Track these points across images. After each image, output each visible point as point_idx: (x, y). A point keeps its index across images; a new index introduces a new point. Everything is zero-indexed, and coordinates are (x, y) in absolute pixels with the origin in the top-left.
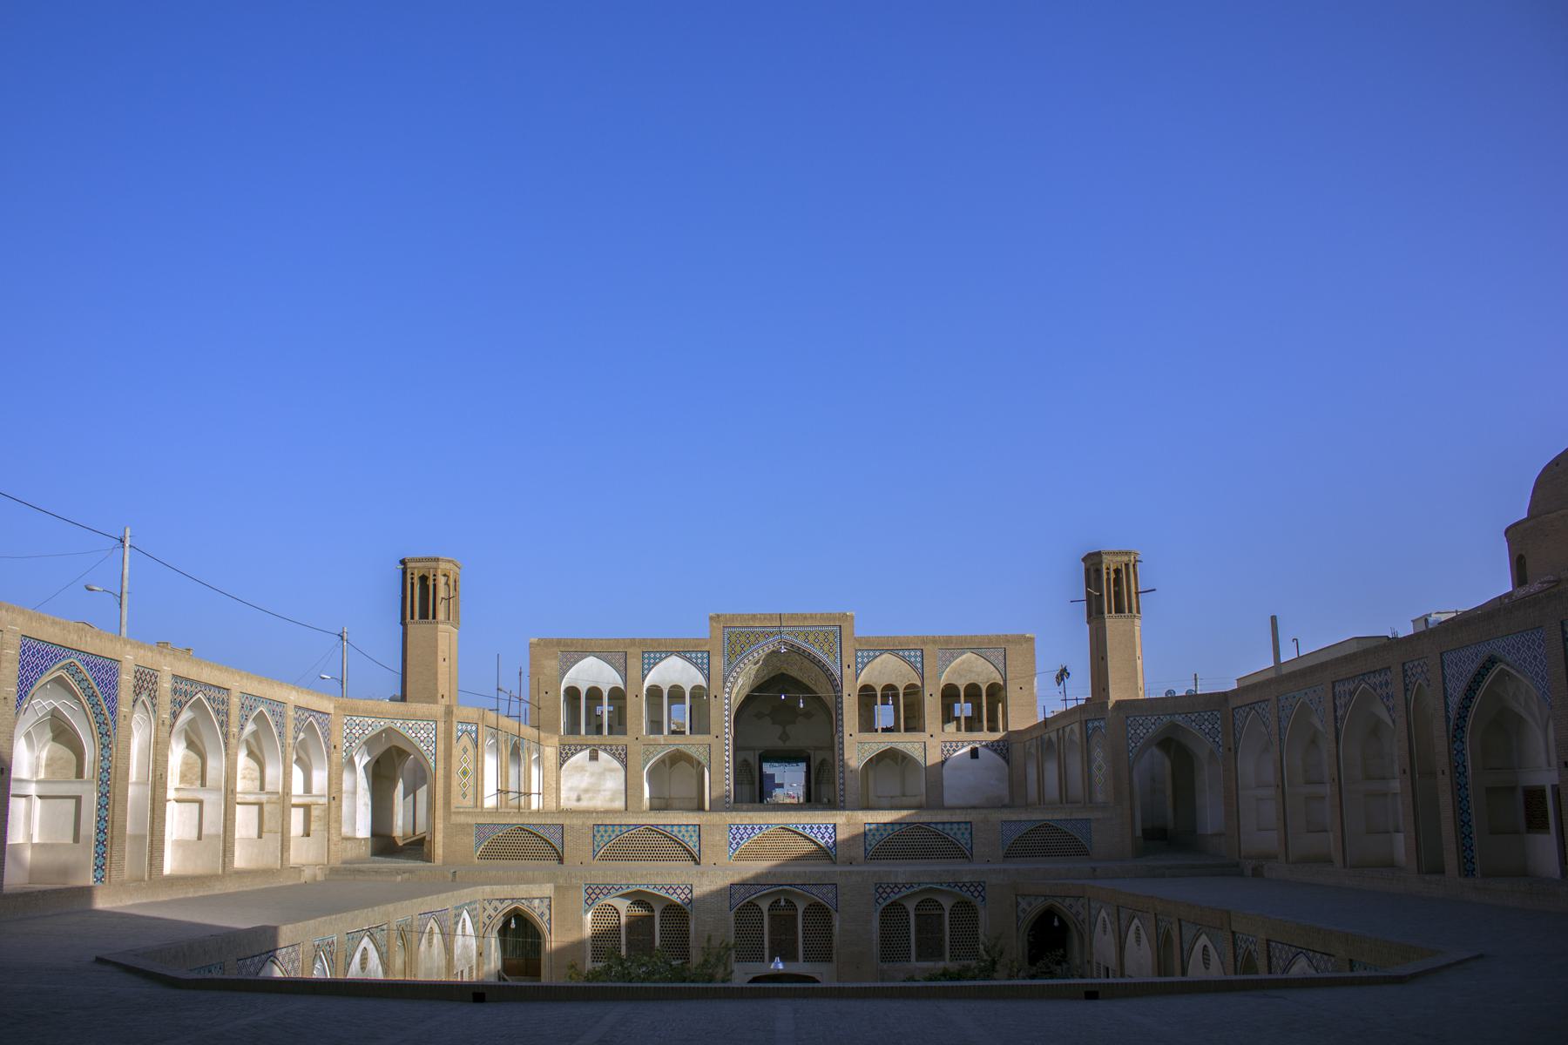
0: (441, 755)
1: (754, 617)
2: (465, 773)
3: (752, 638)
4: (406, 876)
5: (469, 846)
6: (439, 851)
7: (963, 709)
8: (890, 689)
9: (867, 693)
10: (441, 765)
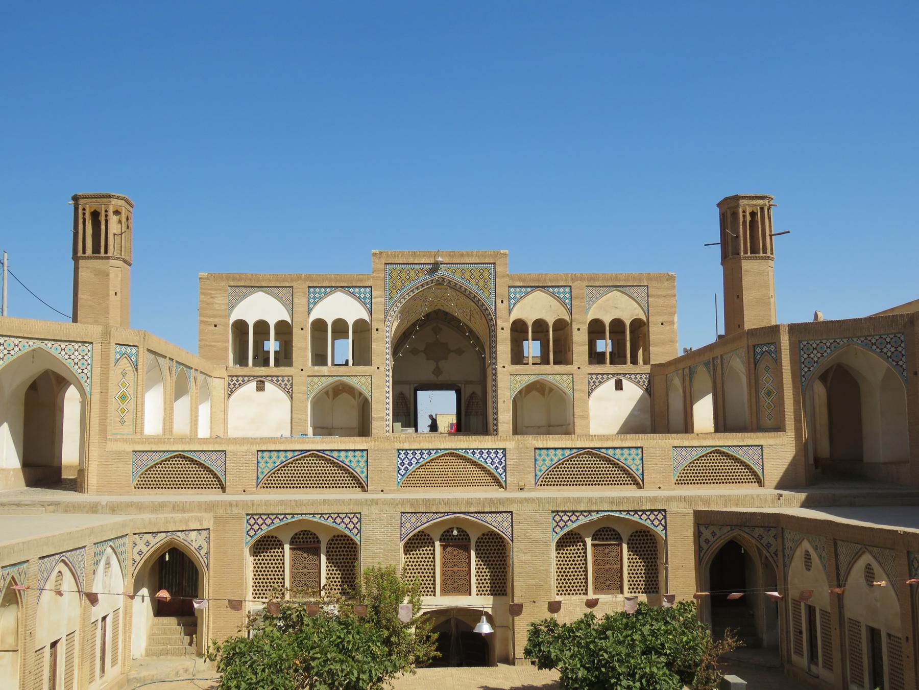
0: (96, 378)
1: (414, 254)
2: (123, 398)
3: (412, 274)
5: (127, 471)
7: (604, 346)
8: (540, 327)
9: (519, 329)
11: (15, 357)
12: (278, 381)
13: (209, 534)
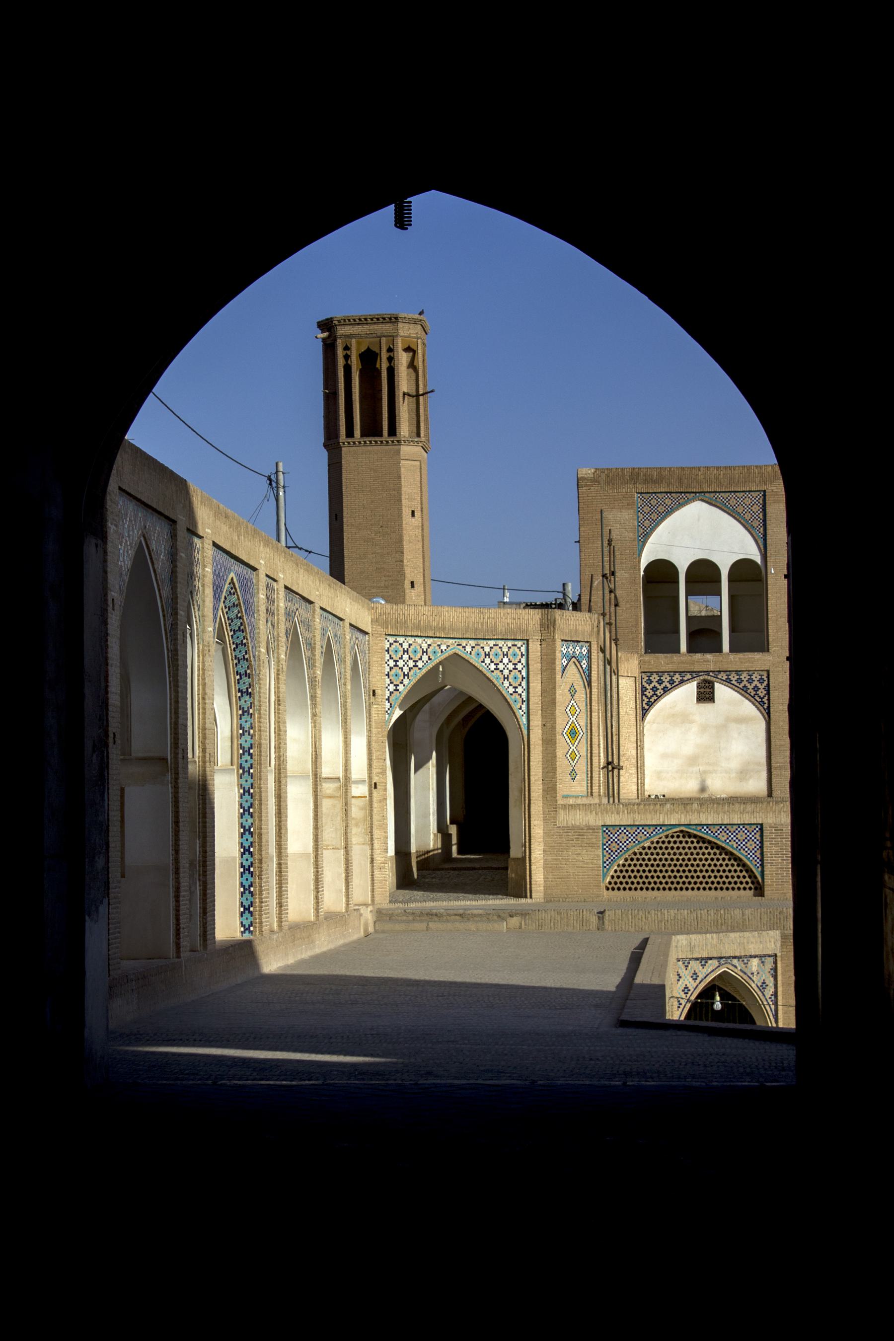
2: (573, 733)
4: (515, 921)
5: (590, 863)
6: (538, 876)
10: (537, 721)
11: (424, 671)
12: (740, 681)
13: (775, 963)
